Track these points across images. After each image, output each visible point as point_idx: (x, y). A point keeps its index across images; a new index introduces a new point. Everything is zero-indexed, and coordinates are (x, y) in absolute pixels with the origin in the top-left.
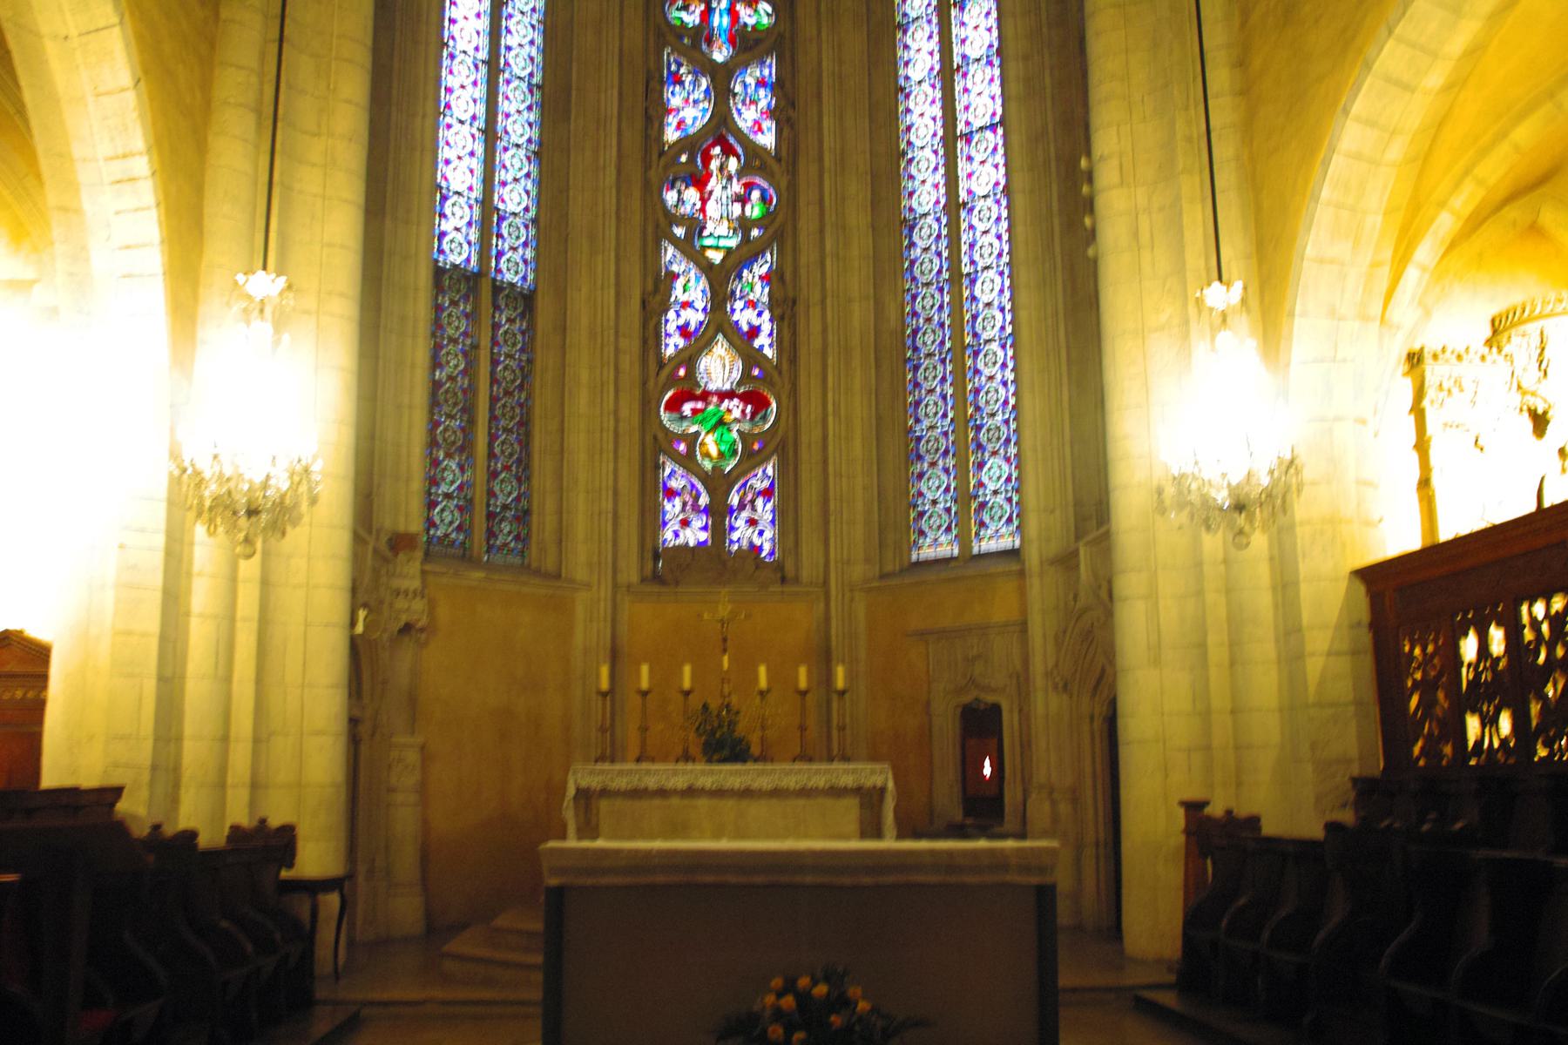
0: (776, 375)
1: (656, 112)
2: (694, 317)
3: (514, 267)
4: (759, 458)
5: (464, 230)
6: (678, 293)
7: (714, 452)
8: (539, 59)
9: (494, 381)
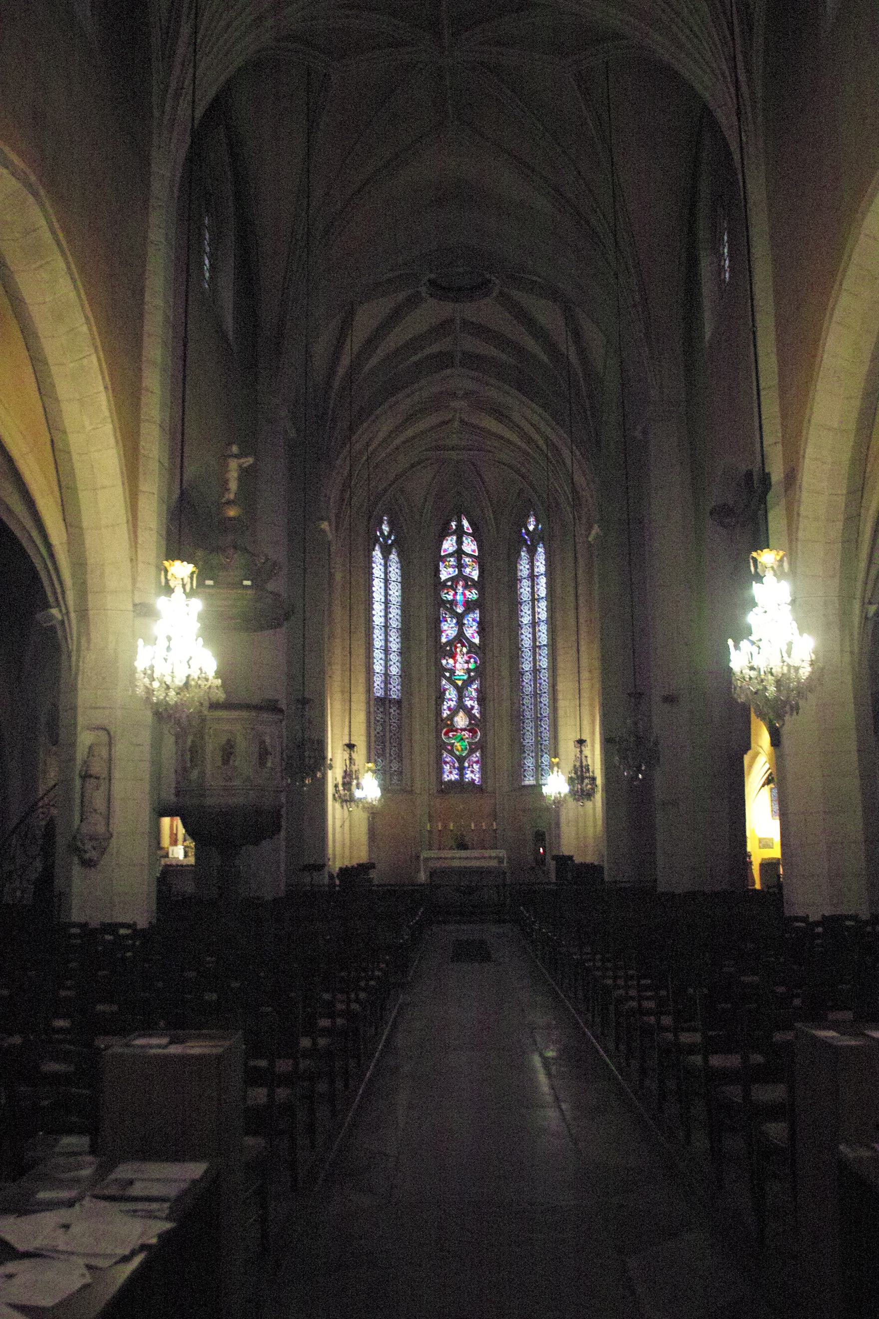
1: (439, 632)
3: (394, 695)
6: (447, 696)
7: (459, 748)
9: (390, 731)
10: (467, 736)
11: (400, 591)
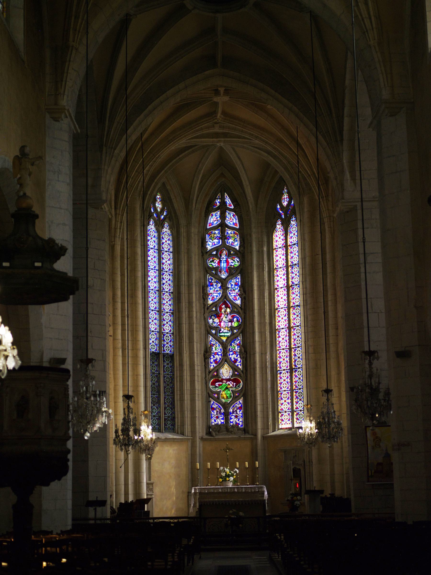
0: (242, 374)
1: (205, 295)
2: (218, 357)
3: (168, 350)
4: (237, 399)
5: (155, 341)
7: (225, 396)
8: (172, 284)
10: (231, 385)
11: (171, 261)
